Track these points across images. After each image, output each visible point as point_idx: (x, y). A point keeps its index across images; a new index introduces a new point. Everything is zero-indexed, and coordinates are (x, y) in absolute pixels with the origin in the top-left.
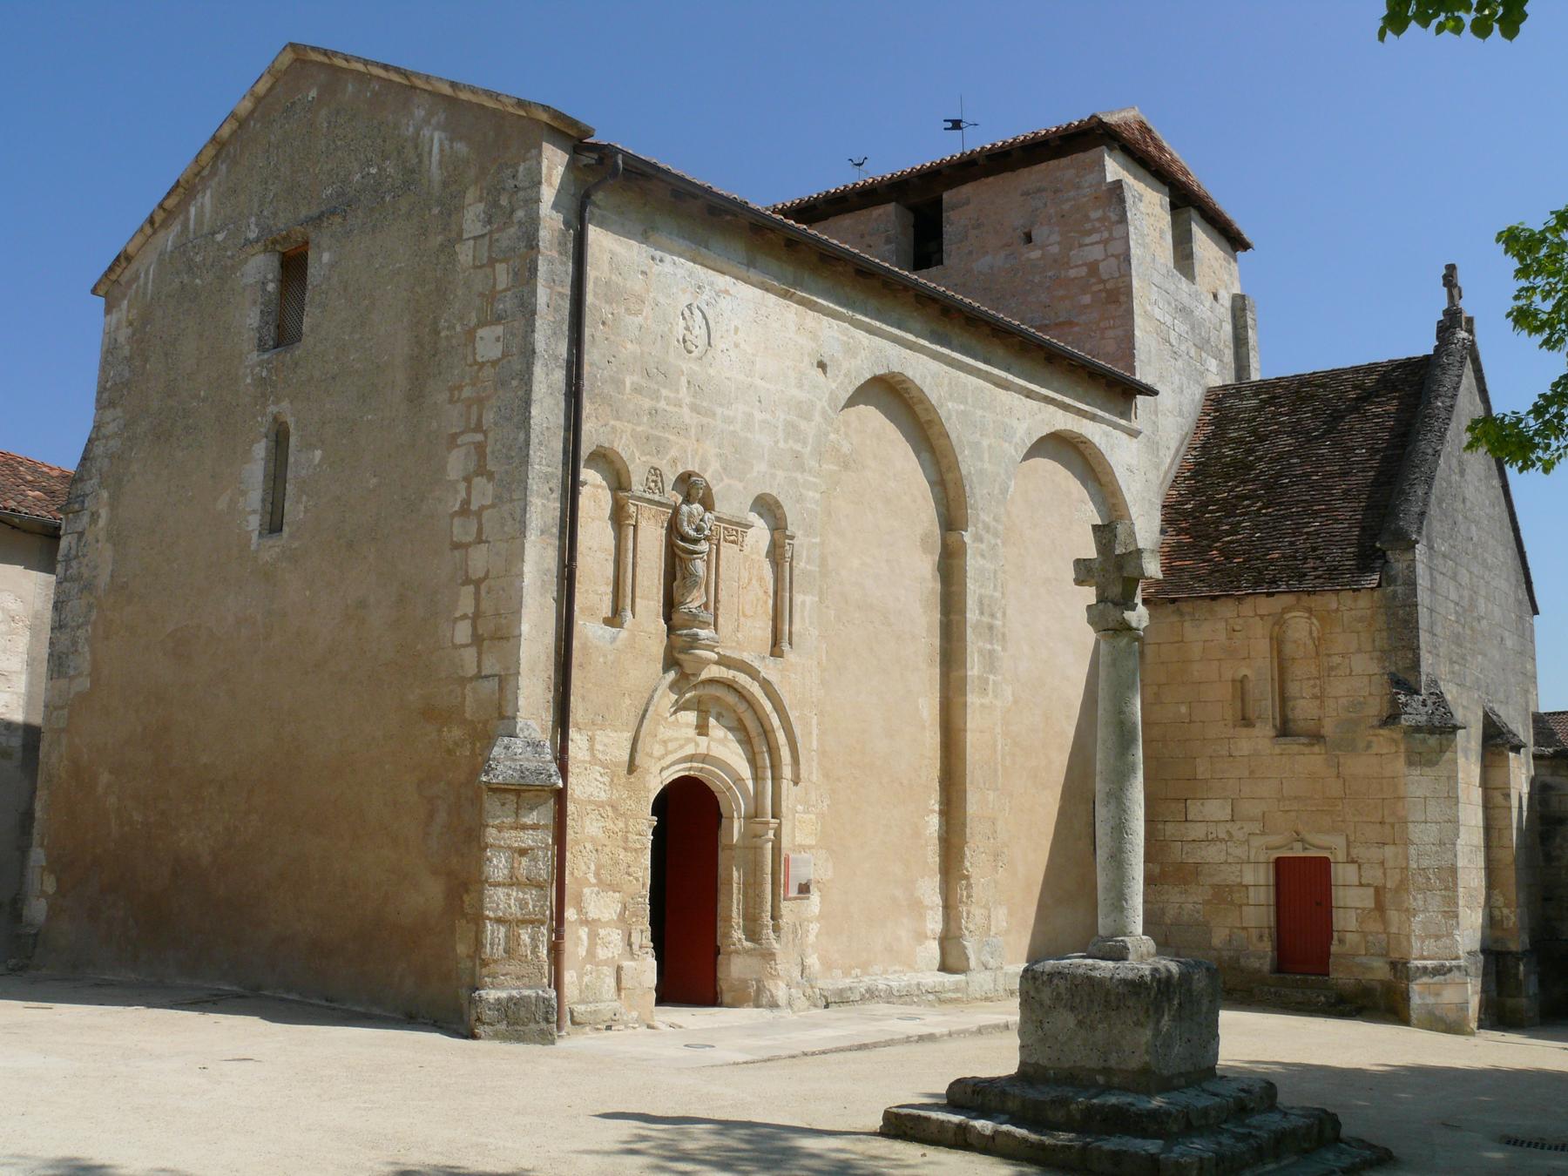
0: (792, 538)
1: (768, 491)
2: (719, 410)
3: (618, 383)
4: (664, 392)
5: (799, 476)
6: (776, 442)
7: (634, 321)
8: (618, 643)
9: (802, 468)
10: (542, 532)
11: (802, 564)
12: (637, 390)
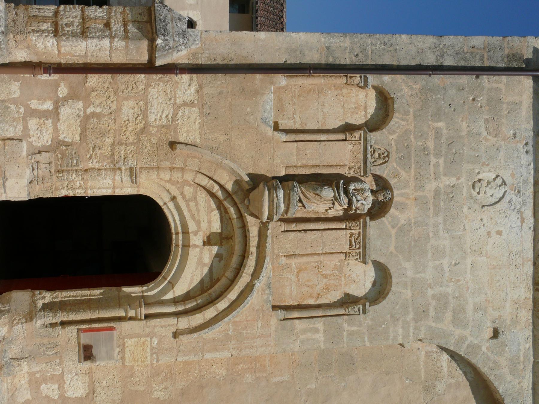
0: (364, 312)
1: (394, 280)
2: (440, 219)
3: (437, 115)
4: (441, 161)
5: (411, 316)
6: (430, 286)
7: (480, 126)
8: (263, 126)
10: (328, 48)
11: (346, 327)
12: (438, 133)
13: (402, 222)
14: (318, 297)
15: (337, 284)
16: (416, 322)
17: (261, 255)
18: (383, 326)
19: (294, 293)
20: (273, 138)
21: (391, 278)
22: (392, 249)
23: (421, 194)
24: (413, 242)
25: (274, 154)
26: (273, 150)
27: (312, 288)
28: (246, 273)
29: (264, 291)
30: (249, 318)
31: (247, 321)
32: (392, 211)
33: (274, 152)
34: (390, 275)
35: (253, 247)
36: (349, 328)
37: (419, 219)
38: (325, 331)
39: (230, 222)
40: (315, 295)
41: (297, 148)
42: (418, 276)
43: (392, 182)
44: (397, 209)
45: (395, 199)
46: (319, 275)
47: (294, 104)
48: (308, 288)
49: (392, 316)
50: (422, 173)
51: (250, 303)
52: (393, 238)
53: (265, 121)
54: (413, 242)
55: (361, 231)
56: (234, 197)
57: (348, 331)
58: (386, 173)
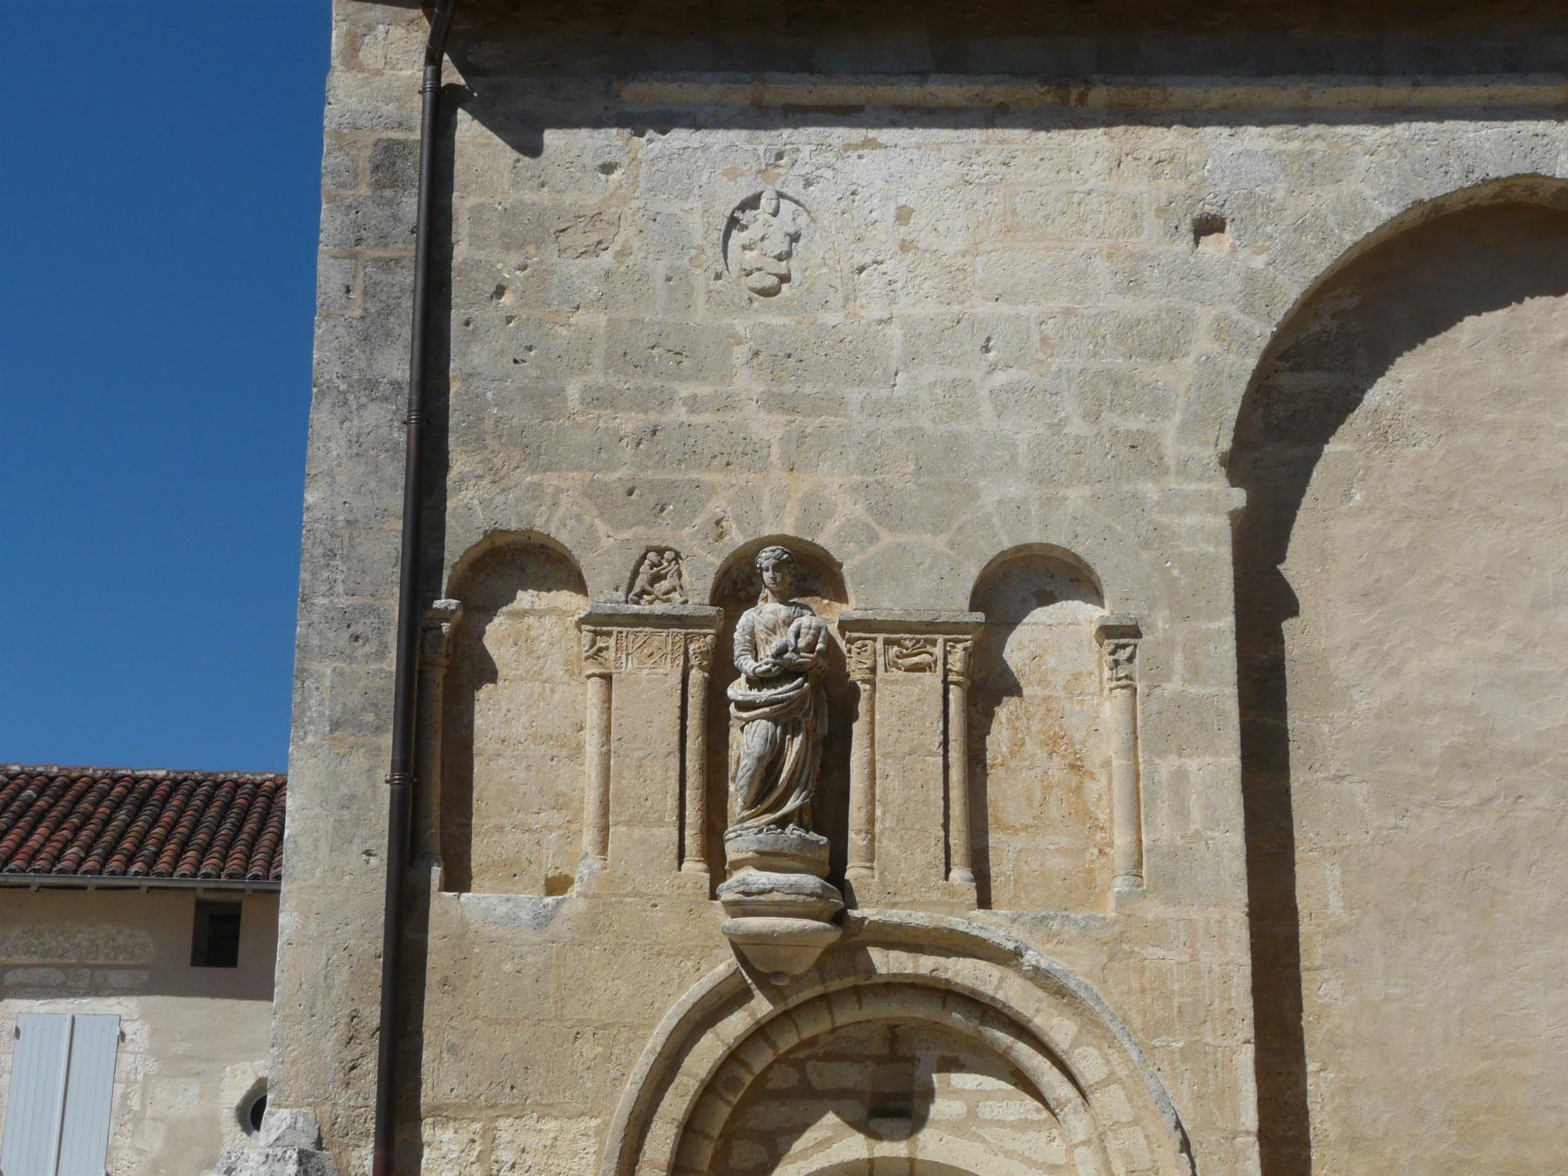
1: (1034, 537)
2: (855, 395)
3: (545, 399)
4: (684, 390)
5: (1150, 490)
6: (1056, 428)
7: (582, 273)
8: (559, 927)
9: (1156, 468)
10: (335, 725)
11: (1170, 688)
12: (597, 399)
13: (859, 511)
14: (1079, 768)
15: (1043, 710)
16: (1166, 472)
17: (944, 944)
18: (1175, 573)
19: (1064, 841)
20: (594, 896)
21: (1029, 546)
22: (940, 543)
23: (775, 451)
24: (923, 479)
26: (627, 895)
27: (1050, 787)
28: (998, 988)
29: (1051, 936)
30: (1135, 985)
31: (1143, 991)
32: (823, 540)
33: (637, 894)
34: (1018, 549)
35: (916, 966)
36: (1177, 678)
37: (852, 458)
38: (1180, 752)
39: (843, 1032)
40: (1075, 780)
41: (629, 823)
42: (1024, 462)
43: (737, 539)
44: (819, 527)
45: (789, 528)
46: (1013, 764)
47: (500, 829)
48: (1052, 800)
49: (1146, 545)
50: (717, 449)
51: (1087, 981)
53: (543, 920)
54: (923, 479)
55: (881, 637)
56: (793, 1002)
57: (1184, 681)
58: (710, 558)
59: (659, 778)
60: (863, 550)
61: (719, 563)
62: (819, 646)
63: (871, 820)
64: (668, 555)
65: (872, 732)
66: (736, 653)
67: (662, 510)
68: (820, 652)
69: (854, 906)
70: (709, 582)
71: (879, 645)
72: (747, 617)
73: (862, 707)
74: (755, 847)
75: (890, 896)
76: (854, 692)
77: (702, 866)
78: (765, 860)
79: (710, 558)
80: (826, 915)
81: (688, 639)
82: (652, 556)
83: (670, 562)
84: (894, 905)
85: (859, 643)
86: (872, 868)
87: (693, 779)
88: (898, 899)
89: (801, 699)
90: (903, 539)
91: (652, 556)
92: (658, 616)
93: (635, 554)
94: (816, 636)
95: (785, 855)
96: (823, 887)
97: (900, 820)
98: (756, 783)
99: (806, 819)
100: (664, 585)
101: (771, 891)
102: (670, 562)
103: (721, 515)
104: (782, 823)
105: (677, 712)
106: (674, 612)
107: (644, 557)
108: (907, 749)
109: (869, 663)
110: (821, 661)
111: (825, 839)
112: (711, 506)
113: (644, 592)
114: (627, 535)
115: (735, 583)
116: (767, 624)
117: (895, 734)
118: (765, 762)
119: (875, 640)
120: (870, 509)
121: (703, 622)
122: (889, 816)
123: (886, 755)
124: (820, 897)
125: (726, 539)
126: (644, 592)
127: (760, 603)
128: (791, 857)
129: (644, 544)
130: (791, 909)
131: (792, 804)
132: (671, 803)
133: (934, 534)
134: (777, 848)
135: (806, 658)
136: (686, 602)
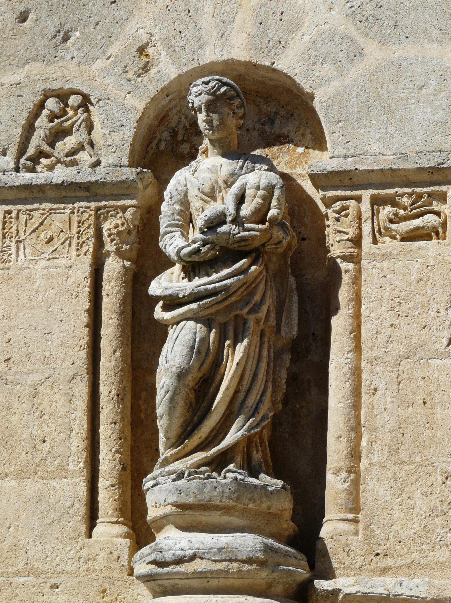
13: (337, 18)
25: (37, 573)
26: (18, 574)
32: (288, 63)
33: (31, 571)
43: (167, 69)
52: (406, 51)
55: (367, 195)
58: (131, 101)
59: (61, 411)
60: (341, 73)
61: (141, 106)
62: (273, 212)
63: (355, 455)
64: (74, 100)
65: (356, 330)
66: (162, 230)
67: (66, 39)
68: (274, 222)
69: (328, 574)
70: (129, 134)
71: (365, 206)
72: (182, 179)
73: (344, 294)
74: (173, 498)
75: (378, 558)
76: (335, 274)
77: (121, 529)
78: (190, 516)
79: (131, 101)
80: (279, 589)
81: (99, 217)
82: (52, 104)
83: (76, 109)
84: (384, 571)
85: (337, 206)
86: (355, 521)
87: (108, 410)
88: (389, 562)
89: (249, 289)
90: (398, 52)
91: (52, 104)
92: (56, 185)
93: (29, 101)
94: (267, 199)
95: (216, 508)
96: (267, 549)
97: (394, 451)
98: (179, 410)
99: (257, 456)
100: (70, 142)
101: (193, 558)
102: (76, 109)
103: (145, 38)
104: (218, 463)
105: (84, 318)
106: (79, 179)
107: (41, 106)
108: (402, 350)
109: (352, 232)
110: (278, 234)
111: (280, 483)
112: (131, 27)
113: (41, 154)
114: (17, 76)
115: (174, 133)
116: (207, 182)
117: (386, 331)
118: (190, 379)
119: (359, 199)
120: (351, 14)
121: (121, 190)
122: (377, 447)
123: (375, 361)
124: (262, 563)
125: (153, 71)
126: (41, 154)
127: (199, 157)
128: (226, 510)
129: (40, 87)
130: (223, 582)
131: (233, 436)
132: (78, 443)
133: (441, 42)
134: (203, 498)
135: (255, 229)
136: (97, 163)
